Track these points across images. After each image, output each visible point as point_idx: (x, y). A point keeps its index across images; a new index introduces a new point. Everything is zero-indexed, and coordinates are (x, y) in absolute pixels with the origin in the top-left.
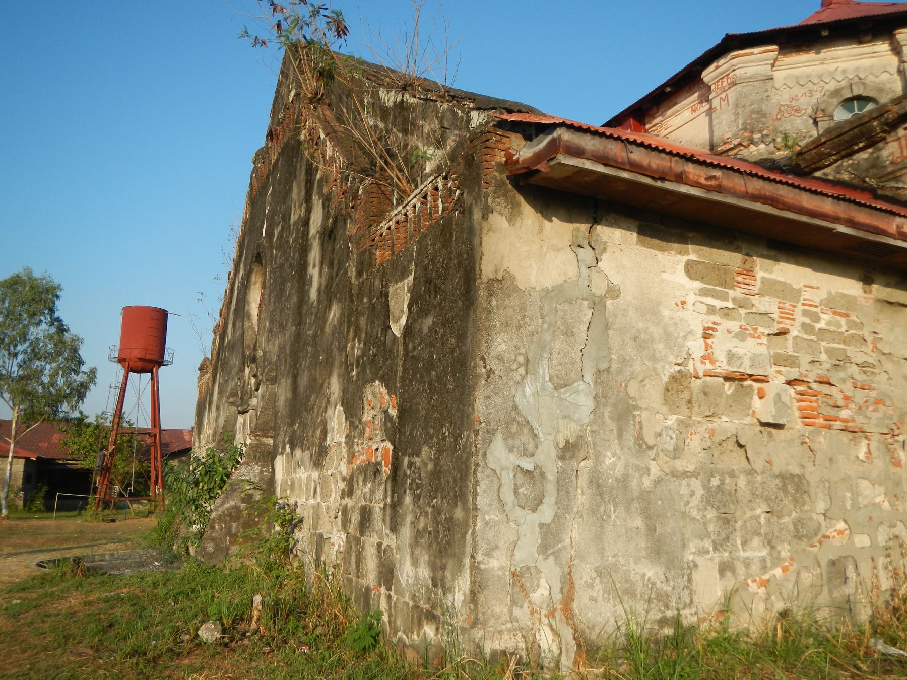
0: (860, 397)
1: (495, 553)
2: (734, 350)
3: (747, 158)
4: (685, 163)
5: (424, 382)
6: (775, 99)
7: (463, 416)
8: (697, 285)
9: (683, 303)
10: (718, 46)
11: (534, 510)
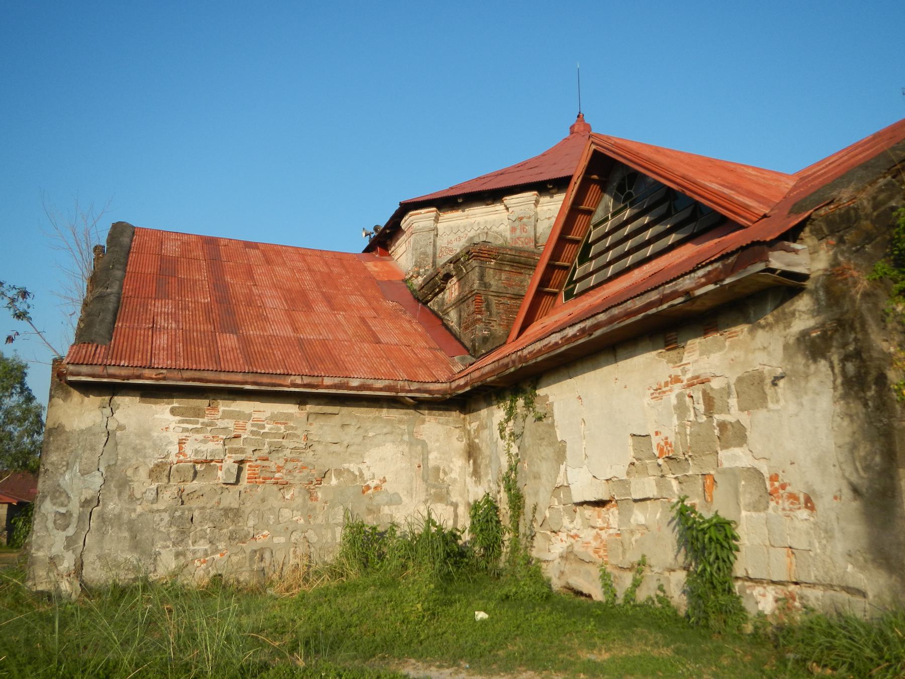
8: (178, 418)
11: (64, 530)
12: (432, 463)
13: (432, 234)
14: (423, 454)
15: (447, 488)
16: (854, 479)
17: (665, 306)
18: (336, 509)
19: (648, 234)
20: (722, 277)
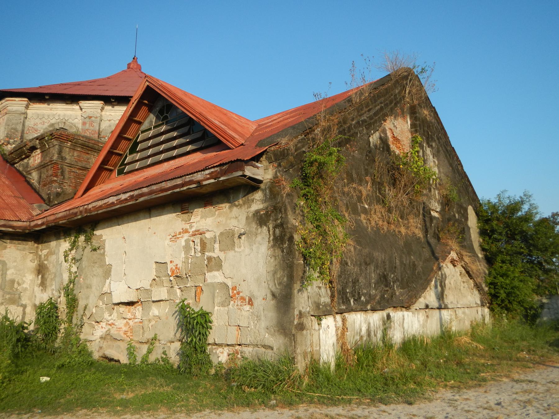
12: (9, 277)
13: (23, 116)
14: (3, 271)
15: (19, 294)
16: (273, 289)
17: (185, 188)
19: (175, 143)
20: (219, 176)
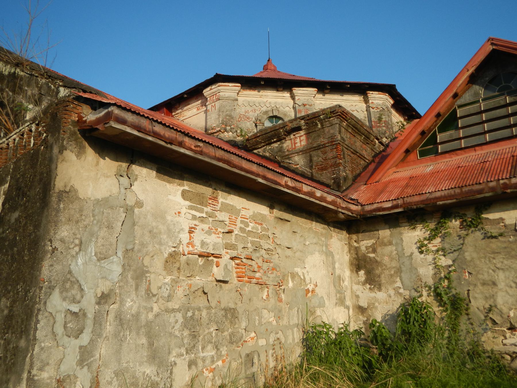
0: (265, 266)
1: (46, 368)
2: (205, 240)
3: (223, 138)
4: (184, 137)
5: (8, 255)
6: (238, 111)
7: (32, 277)
8: (188, 203)
9: (179, 213)
10: (212, 78)
11: (77, 337)
18: (293, 310)
